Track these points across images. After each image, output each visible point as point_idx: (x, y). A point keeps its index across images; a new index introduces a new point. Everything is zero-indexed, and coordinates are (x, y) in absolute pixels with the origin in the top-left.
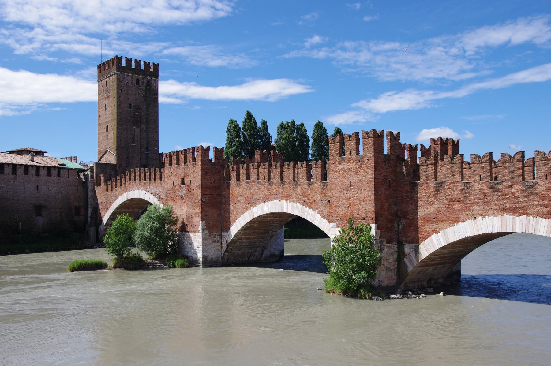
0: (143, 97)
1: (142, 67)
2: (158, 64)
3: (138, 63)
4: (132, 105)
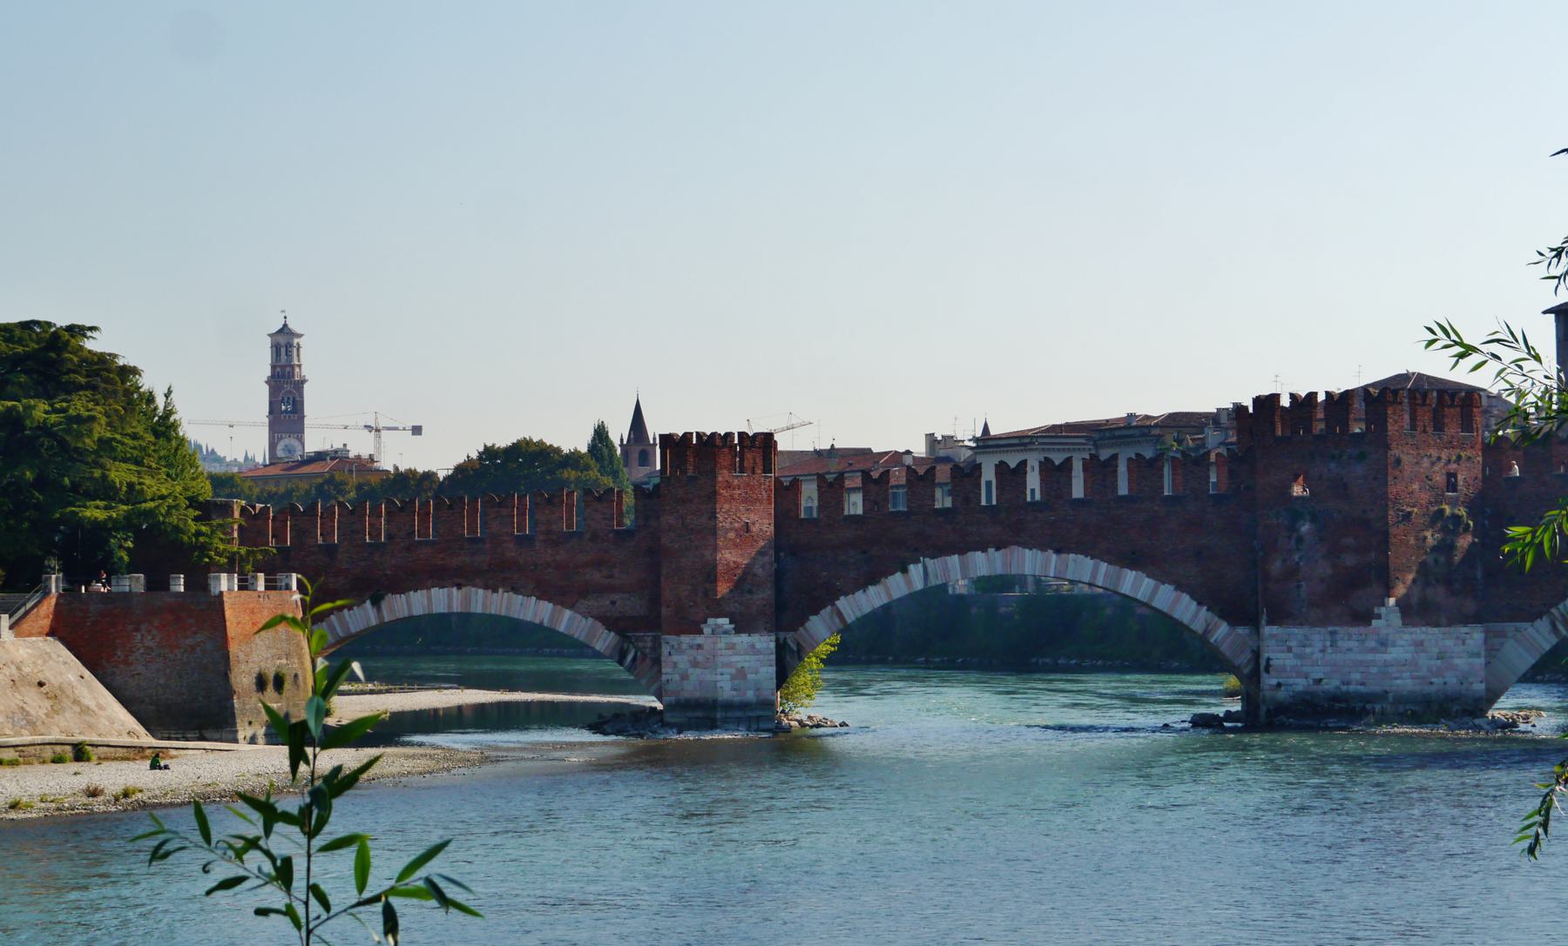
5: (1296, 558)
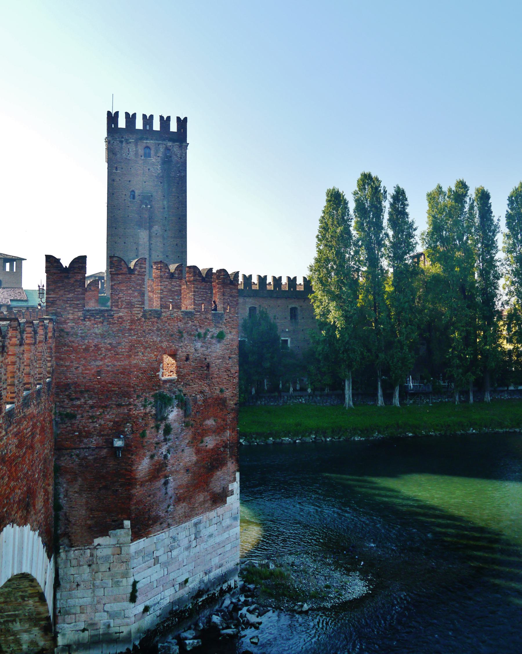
0: (157, 177)
1: (156, 126)
2: (186, 119)
3: (148, 120)
4: (136, 194)
5: (164, 450)
